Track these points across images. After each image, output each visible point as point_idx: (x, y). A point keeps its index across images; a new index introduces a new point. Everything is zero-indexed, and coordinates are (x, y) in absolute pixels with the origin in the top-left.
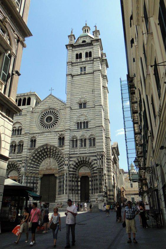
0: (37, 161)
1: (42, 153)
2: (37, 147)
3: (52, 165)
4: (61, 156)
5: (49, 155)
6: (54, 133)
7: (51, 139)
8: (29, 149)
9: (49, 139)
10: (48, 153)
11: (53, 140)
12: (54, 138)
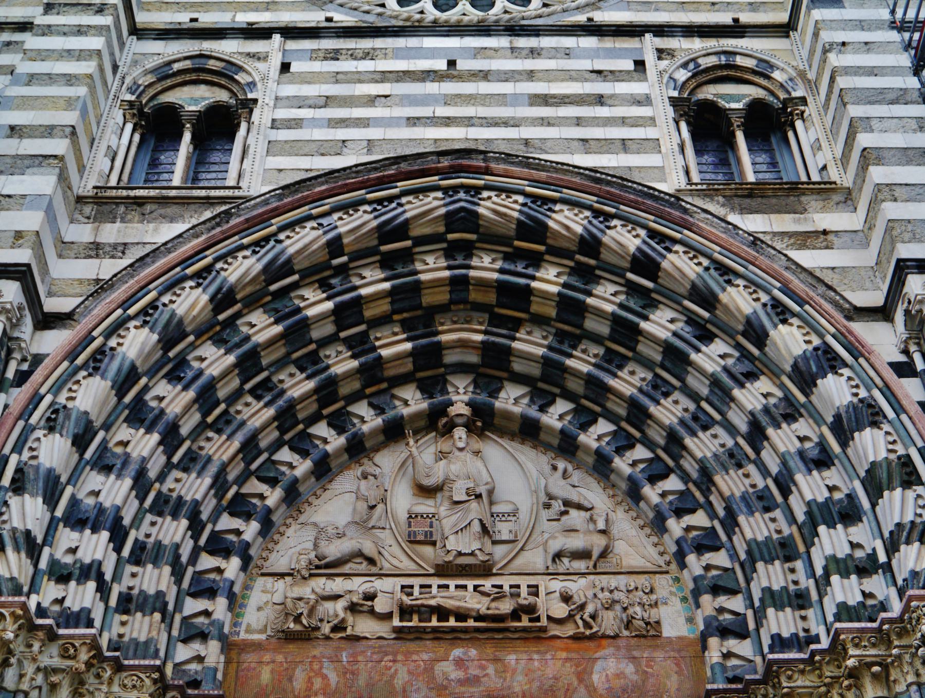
0: (221, 449)
1: (348, 313)
2: (256, 185)
3: (535, 559)
4: (790, 341)
5: (460, 395)
6: (589, 42)
7: (545, 100)
8: (102, 204)
9: (501, 99)
10: (461, 335)
11: (579, 122)
12: (600, 100)
